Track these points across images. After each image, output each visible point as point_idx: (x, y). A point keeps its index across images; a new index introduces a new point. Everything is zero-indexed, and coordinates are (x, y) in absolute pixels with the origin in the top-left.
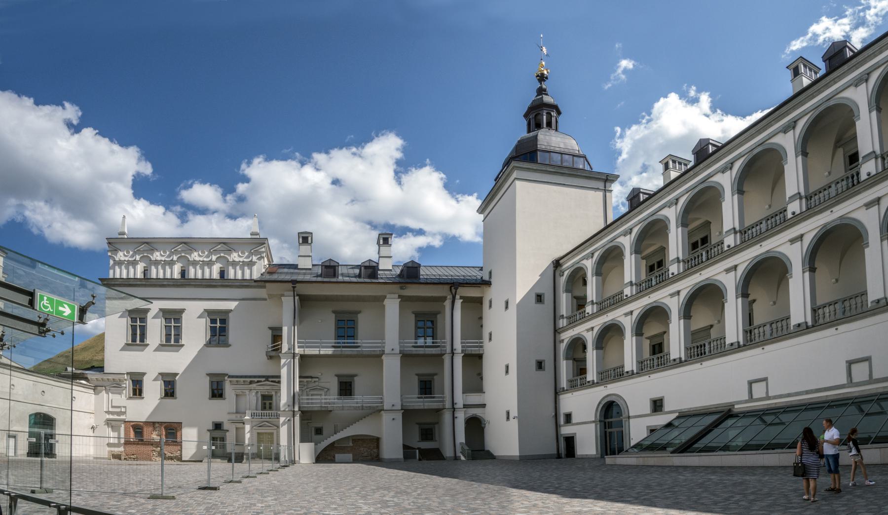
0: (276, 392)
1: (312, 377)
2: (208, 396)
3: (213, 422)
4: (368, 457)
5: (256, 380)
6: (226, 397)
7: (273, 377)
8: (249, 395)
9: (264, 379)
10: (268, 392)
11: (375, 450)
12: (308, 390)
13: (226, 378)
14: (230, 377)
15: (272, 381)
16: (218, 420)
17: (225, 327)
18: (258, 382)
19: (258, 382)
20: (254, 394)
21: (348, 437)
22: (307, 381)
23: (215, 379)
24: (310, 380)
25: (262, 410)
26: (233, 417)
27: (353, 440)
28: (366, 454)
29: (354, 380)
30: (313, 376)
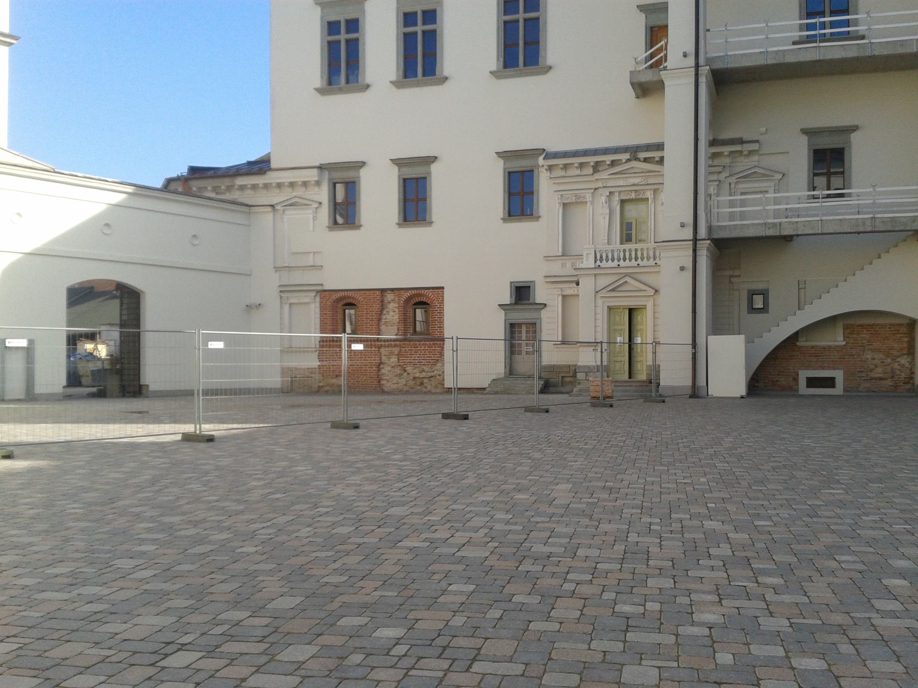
0: (655, 191)
1: (741, 141)
2: (501, 215)
3: (511, 283)
4: (883, 382)
5: (608, 158)
6: (541, 214)
7: (648, 147)
8: (592, 203)
9: (627, 156)
10: (636, 191)
11: (904, 360)
12: (733, 180)
13: (541, 161)
14: (550, 156)
15: (646, 160)
16: (522, 277)
17: (537, 19)
18: (613, 163)
19: (613, 163)
20: (603, 199)
21: (832, 320)
22: (731, 153)
23: (518, 165)
24: (737, 148)
25: (621, 243)
26: (556, 268)
27: (846, 327)
28: (878, 372)
29: (849, 142)
30: (746, 137)
